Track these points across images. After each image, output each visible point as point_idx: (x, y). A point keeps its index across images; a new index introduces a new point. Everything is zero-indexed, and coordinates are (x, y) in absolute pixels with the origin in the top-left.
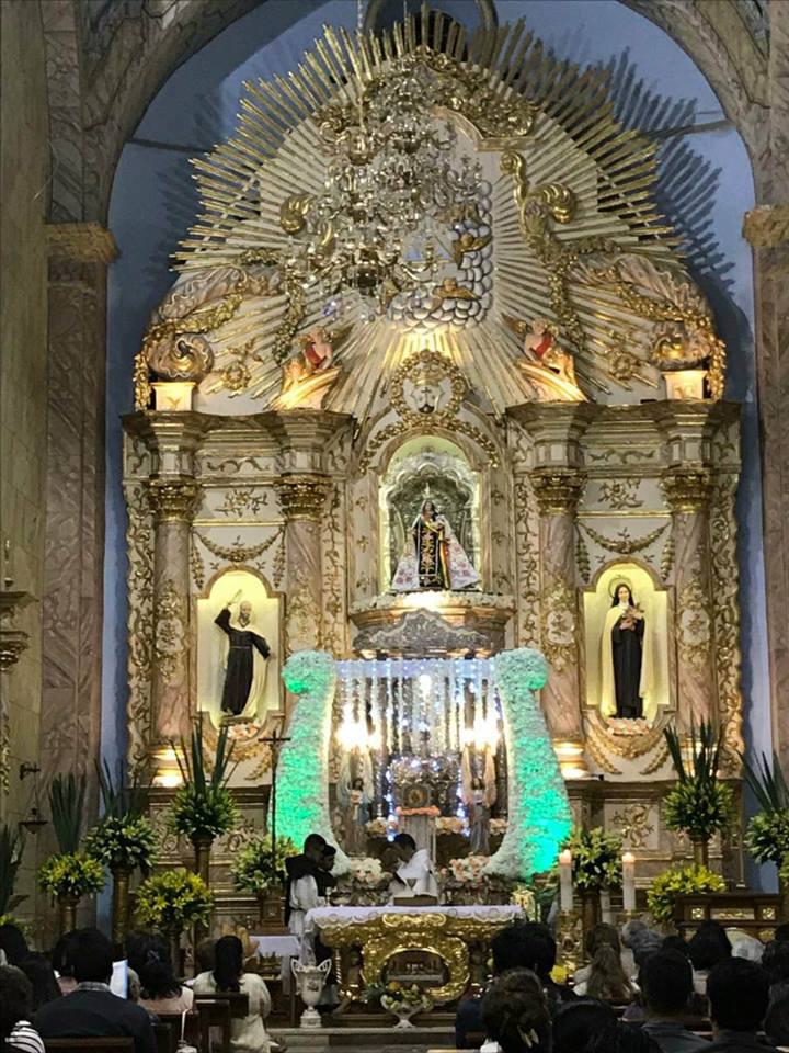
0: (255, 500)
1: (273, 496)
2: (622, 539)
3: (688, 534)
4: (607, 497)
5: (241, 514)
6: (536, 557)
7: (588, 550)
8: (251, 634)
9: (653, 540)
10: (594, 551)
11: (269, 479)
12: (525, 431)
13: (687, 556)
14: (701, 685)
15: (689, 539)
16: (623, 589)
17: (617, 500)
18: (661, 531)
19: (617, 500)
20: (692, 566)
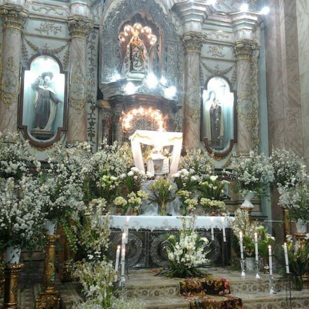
0: (56, 28)
1: (64, 27)
2: (216, 69)
3: (245, 68)
4: (210, 51)
5: (48, 34)
6: (181, 72)
7: (203, 72)
8: (50, 92)
9: (228, 71)
10: (205, 72)
11: (64, 19)
12: (179, 19)
13: (244, 79)
14: (249, 131)
15: (245, 71)
16: (213, 94)
17: (214, 53)
18: (231, 68)
19: (214, 53)
20: (246, 83)
